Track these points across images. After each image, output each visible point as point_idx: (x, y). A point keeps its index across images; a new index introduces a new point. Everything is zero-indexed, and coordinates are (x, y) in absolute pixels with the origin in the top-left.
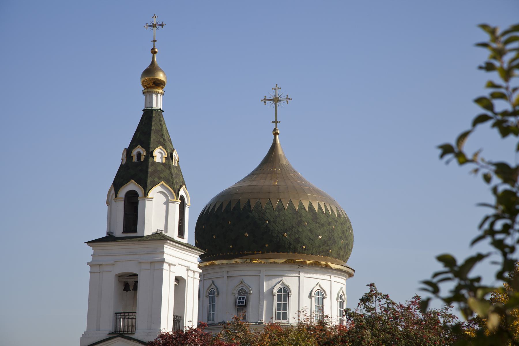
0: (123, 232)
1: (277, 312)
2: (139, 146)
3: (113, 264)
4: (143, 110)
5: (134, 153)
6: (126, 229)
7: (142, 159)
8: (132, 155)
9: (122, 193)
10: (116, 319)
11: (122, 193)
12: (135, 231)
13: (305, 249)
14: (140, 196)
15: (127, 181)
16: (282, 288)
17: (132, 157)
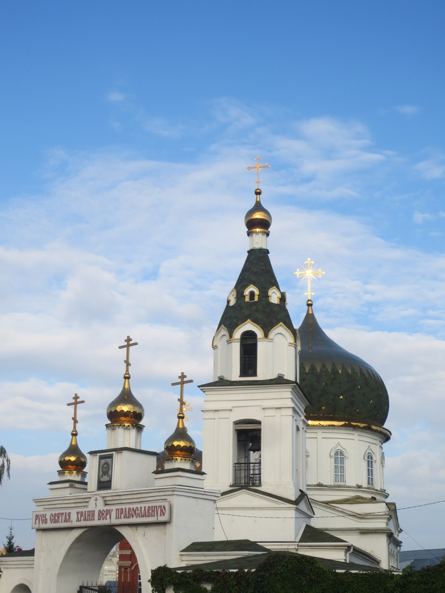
0: (241, 376)
1: (335, 474)
2: (252, 285)
3: (231, 410)
4: (248, 252)
5: (247, 292)
6: (243, 373)
7: (256, 299)
8: (244, 295)
9: (238, 334)
10: (236, 470)
11: (238, 334)
12: (255, 374)
13: (358, 412)
14: (258, 337)
15: (243, 321)
16: (338, 451)
17: (245, 296)
